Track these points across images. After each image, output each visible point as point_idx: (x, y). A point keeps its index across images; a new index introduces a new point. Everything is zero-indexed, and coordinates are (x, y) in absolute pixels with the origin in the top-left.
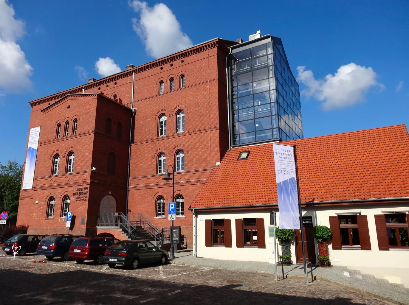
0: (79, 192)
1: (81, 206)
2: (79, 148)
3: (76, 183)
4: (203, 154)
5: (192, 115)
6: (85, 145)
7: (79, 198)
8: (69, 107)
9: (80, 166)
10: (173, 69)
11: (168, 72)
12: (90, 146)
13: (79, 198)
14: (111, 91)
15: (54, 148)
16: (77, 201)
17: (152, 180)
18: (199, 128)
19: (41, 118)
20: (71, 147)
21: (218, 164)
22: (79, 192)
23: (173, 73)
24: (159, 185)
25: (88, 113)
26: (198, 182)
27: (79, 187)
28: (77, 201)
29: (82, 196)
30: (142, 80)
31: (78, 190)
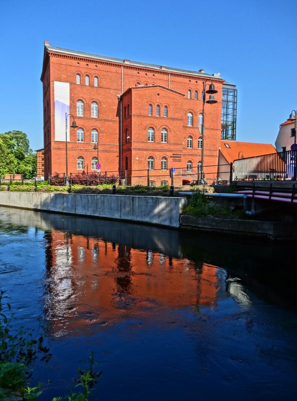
0: (174, 156)
1: (177, 164)
2: (171, 127)
3: (172, 150)
4: (213, 142)
5: (208, 118)
6: (176, 127)
7: (175, 159)
8: (158, 94)
9: (174, 140)
10: (198, 86)
11: (194, 86)
12: (180, 128)
13: (175, 159)
14: (150, 80)
15: (148, 122)
16: (173, 161)
17: (185, 151)
18: (212, 127)
19: (68, 75)
20: (165, 125)
21: (220, 148)
22: (174, 156)
23: (198, 88)
24: (190, 155)
25: (176, 105)
26: (210, 156)
27: (174, 153)
28: (173, 161)
29: (177, 158)
30: (176, 83)
31: (173, 154)
